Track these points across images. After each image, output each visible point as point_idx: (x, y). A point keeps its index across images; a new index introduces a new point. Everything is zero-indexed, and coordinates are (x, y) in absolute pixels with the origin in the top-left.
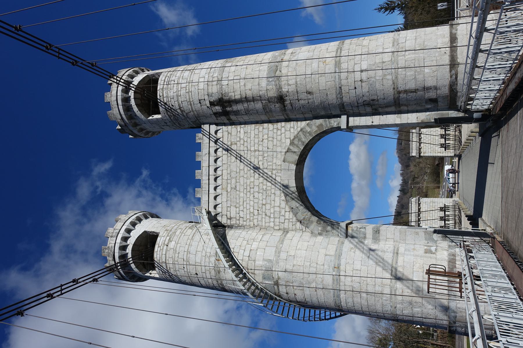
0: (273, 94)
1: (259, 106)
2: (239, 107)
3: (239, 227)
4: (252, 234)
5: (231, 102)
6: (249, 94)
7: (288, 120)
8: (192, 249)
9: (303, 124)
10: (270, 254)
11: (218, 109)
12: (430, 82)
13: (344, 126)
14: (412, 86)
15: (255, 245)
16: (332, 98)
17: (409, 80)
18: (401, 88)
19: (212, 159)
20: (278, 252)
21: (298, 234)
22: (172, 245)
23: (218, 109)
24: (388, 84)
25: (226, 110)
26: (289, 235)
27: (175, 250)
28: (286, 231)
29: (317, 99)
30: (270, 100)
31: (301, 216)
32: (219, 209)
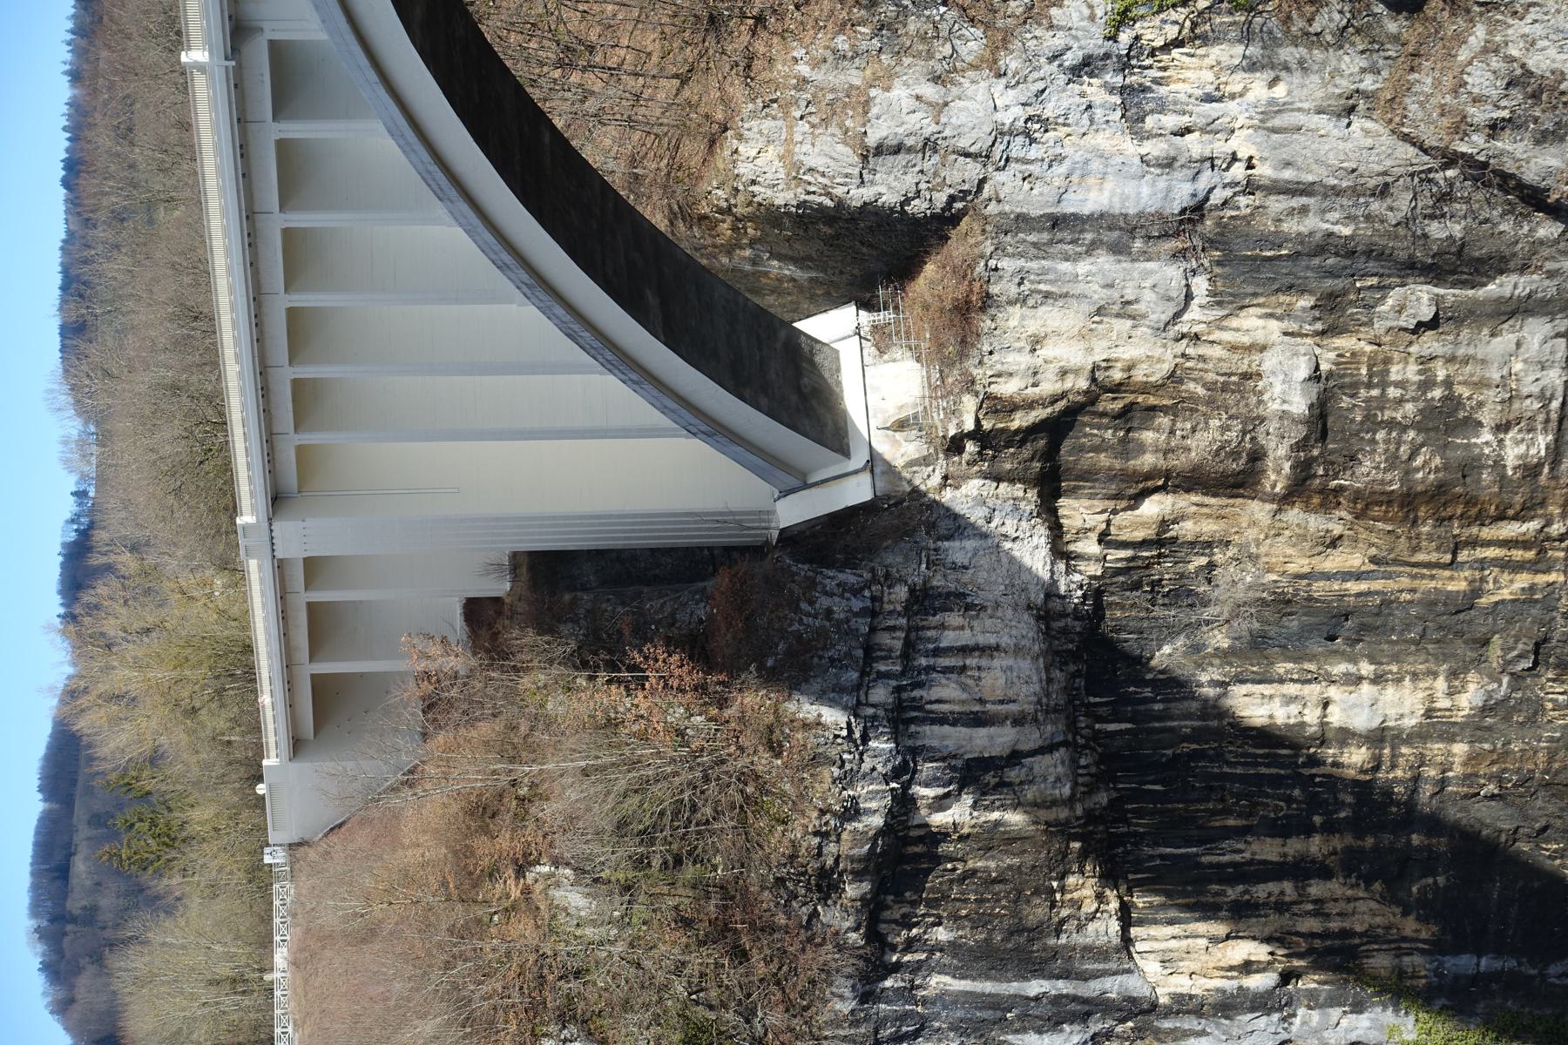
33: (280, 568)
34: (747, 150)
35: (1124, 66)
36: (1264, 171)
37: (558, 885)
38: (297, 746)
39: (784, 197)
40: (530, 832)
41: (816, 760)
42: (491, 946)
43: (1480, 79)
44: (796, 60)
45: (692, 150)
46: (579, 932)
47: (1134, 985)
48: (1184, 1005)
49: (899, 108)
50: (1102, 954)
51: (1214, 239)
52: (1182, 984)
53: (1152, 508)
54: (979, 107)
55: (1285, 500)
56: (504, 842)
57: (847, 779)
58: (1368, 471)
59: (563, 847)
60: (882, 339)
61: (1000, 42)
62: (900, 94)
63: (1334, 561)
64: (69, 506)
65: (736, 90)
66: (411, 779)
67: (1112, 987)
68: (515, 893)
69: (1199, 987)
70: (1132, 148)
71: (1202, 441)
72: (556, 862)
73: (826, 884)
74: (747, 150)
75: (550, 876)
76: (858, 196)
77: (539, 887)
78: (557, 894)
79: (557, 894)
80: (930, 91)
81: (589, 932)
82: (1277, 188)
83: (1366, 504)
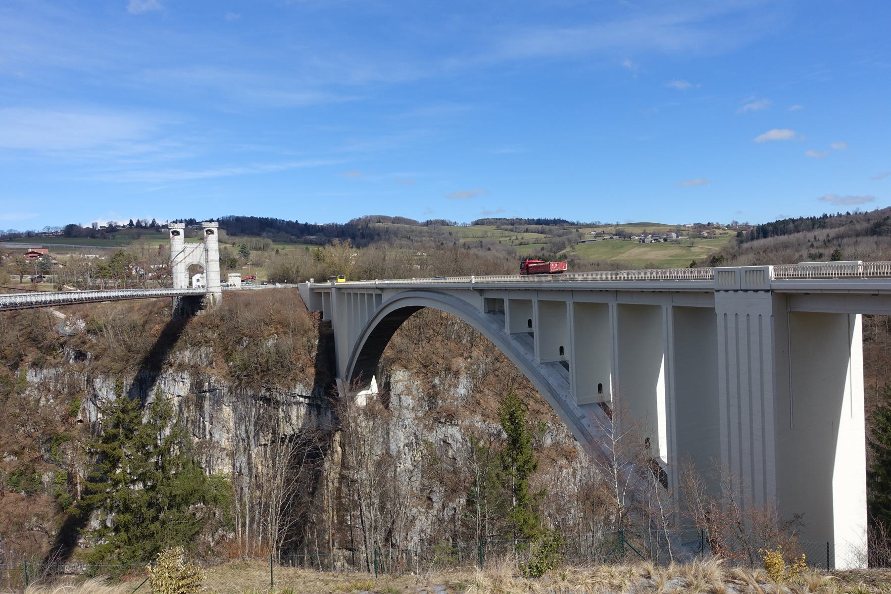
25: (207, 250)
33: (330, 288)
34: (401, 373)
35: (416, 443)
36: (398, 470)
39: (392, 380)
41: (289, 388)
43: (414, 510)
44: (417, 382)
45: (404, 362)
47: (253, 447)
48: (250, 456)
49: (408, 401)
50: (258, 440)
51: (387, 461)
52: (254, 456)
53: (339, 449)
54: (409, 417)
55: (340, 474)
57: (286, 394)
58: (345, 490)
60: (370, 398)
61: (419, 419)
62: (410, 401)
63: (330, 484)
64: (453, 221)
65: (414, 371)
67: (252, 442)
69: (253, 460)
70: (401, 445)
71: (352, 460)
73: (268, 390)
74: (401, 373)
76: (392, 393)
80: (411, 407)
82: (395, 471)
83: (339, 489)
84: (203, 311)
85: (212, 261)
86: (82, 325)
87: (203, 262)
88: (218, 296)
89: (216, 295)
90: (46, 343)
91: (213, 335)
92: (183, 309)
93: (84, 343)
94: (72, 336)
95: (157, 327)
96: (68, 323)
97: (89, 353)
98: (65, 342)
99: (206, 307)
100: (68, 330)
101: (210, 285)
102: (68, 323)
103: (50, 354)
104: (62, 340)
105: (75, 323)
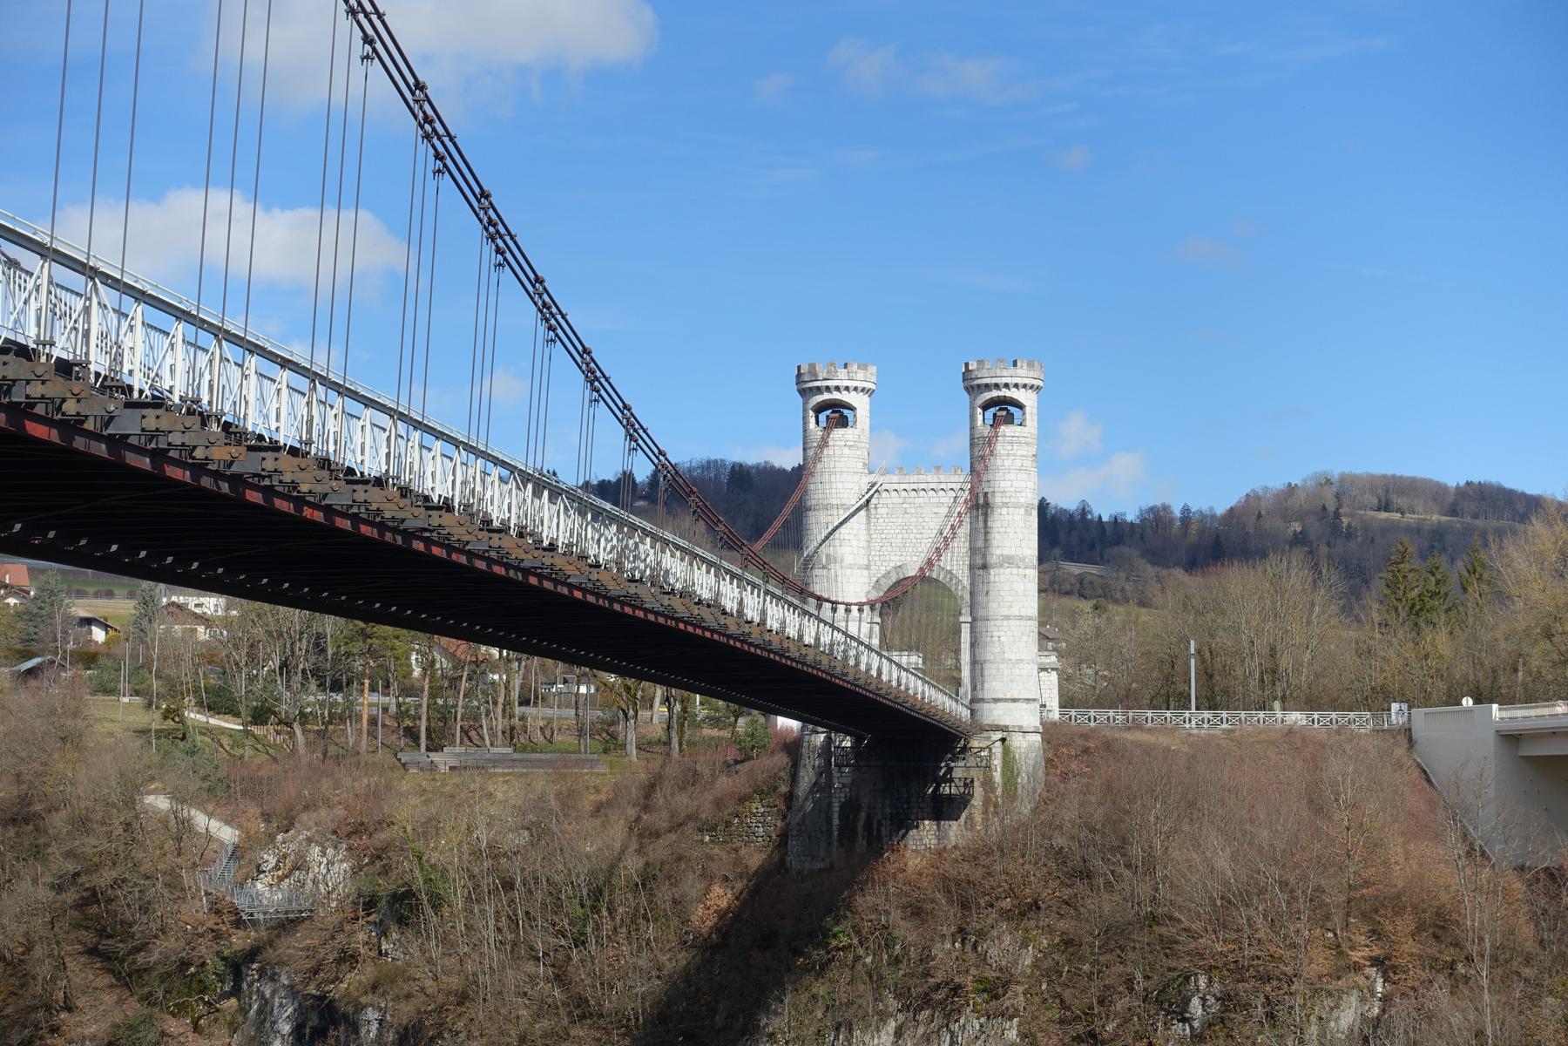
0: (993, 560)
1: (980, 544)
2: (981, 524)
3: (869, 523)
4: (863, 537)
5: (986, 515)
6: (991, 536)
7: (972, 567)
8: (844, 477)
9: (966, 582)
10: (848, 560)
11: (981, 501)
12: (986, 686)
13: (962, 619)
14: (986, 673)
15: (854, 543)
16: (980, 613)
17: (989, 670)
18: (987, 666)
19: (934, 486)
20: (851, 567)
21: (866, 580)
22: (846, 451)
23: (981, 501)
24: (989, 657)
26: (865, 572)
27: (841, 456)
28: (868, 567)
29: (981, 598)
30: (984, 556)
31: (883, 581)
32: (884, 494)
37: (1363, 1000)
38: (1511, 739)
40: (1417, 973)
42: (1302, 928)
46: (1313, 1019)
56: (1409, 946)
59: (1401, 1007)
66: (1475, 853)
68: (1356, 956)
72: (1386, 999)
75: (1373, 993)
77: (1361, 980)
78: (1353, 999)
79: (1353, 999)
81: (1314, 1029)
84: (955, 831)
85: (1009, 561)
86: (332, 871)
87: (956, 563)
88: (1027, 746)
89: (1019, 743)
90: (164, 948)
91: (1012, 950)
92: (850, 808)
93: (348, 958)
94: (286, 924)
95: (721, 897)
96: (270, 860)
97: (372, 1015)
98: (252, 954)
99: (963, 801)
100: (267, 895)
101: (994, 686)
102: (270, 860)
103: (181, 1010)
104: (239, 941)
105: (300, 865)
